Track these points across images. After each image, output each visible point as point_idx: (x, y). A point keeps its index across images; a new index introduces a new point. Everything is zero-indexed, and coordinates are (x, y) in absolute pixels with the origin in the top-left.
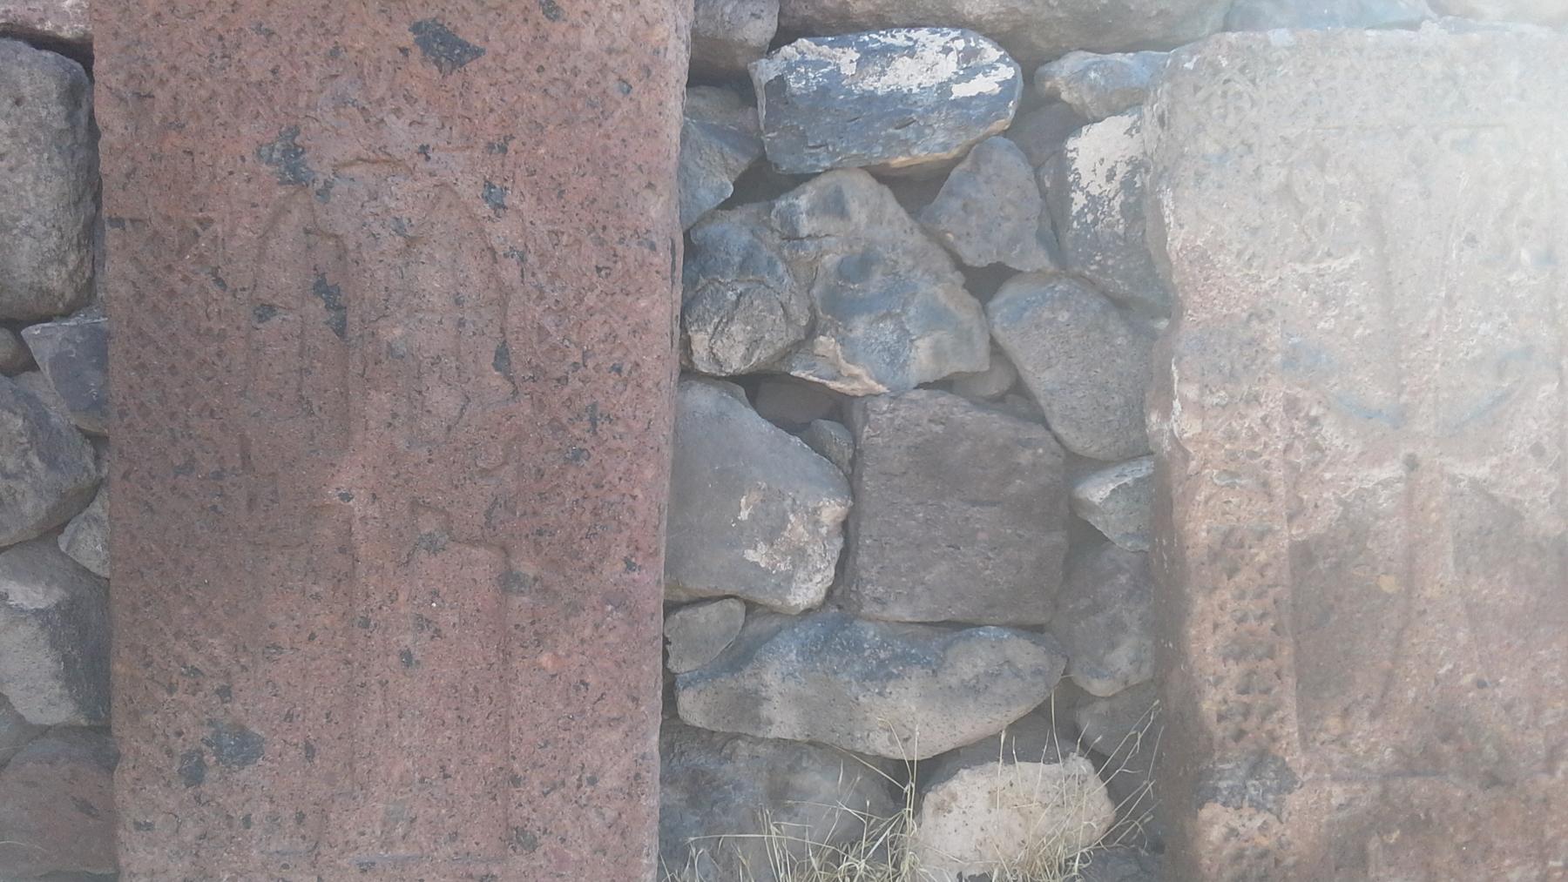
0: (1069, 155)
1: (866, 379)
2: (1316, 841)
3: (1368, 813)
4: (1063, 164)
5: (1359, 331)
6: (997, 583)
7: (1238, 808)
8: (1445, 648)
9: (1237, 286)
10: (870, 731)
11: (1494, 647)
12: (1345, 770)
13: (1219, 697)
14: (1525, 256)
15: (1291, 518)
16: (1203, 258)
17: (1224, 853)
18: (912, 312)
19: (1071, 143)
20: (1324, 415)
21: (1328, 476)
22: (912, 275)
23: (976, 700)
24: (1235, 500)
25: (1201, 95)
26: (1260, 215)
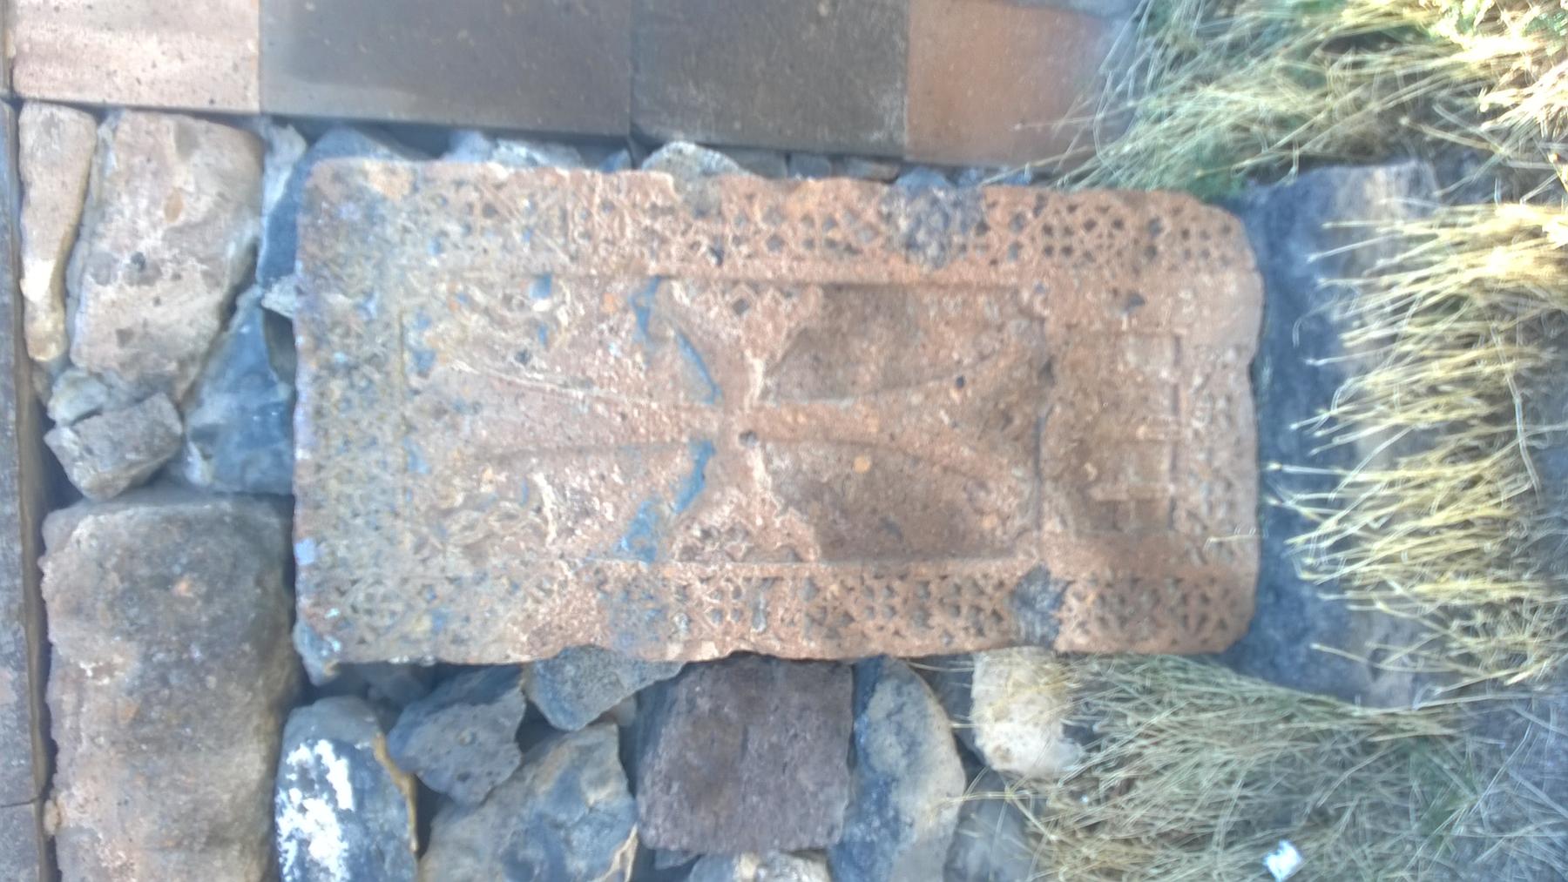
5: (616, 477)
6: (819, 728)
7: (1061, 622)
13: (962, 634)
14: (541, 306)
15: (798, 558)
16: (540, 635)
18: (562, 817)
21: (759, 522)
23: (920, 744)
25: (369, 637)
26: (499, 578)
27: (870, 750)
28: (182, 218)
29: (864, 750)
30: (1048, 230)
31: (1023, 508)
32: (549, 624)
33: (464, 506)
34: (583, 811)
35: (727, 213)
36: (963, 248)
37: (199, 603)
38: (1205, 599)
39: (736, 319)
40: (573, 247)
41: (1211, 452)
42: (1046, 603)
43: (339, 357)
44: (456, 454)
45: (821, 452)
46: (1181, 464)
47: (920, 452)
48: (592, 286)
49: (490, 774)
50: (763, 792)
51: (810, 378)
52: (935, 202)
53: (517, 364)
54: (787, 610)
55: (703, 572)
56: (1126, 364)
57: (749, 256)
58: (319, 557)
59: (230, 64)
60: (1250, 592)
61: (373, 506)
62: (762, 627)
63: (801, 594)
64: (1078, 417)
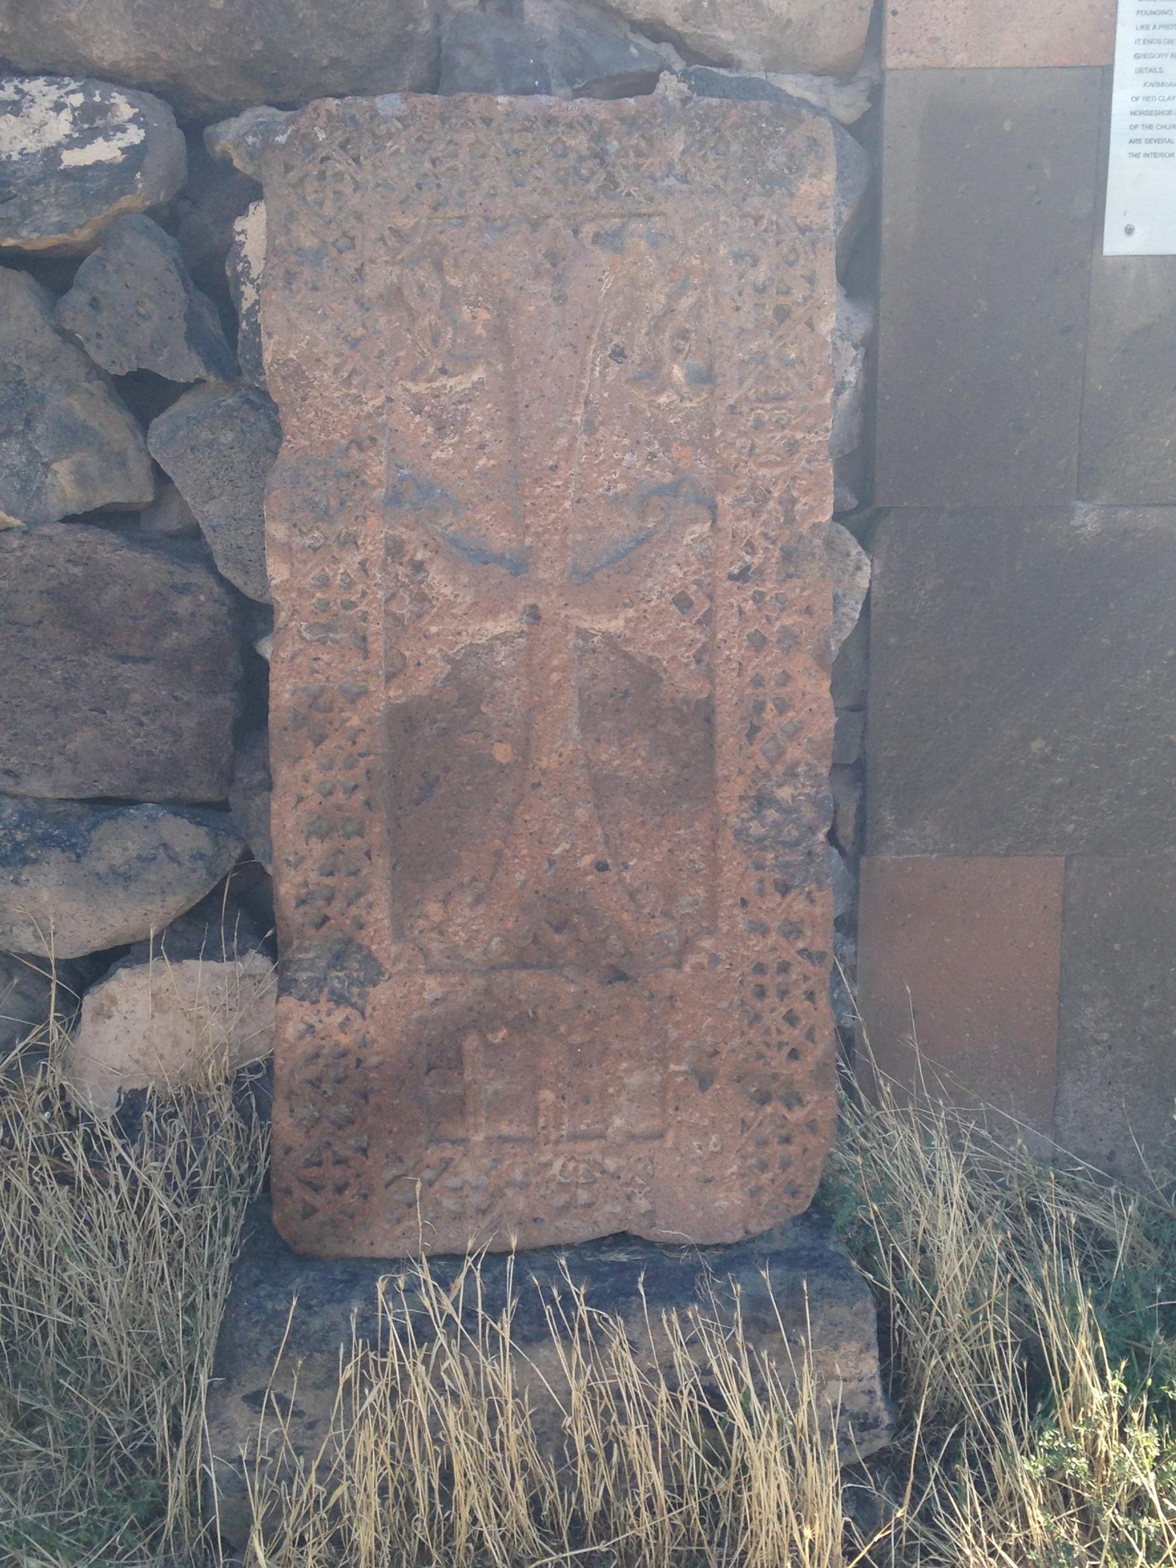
0: (238, 238)
2: (404, 1039)
3: (471, 1009)
4: (229, 248)
5: (482, 462)
6: (150, 753)
9: (335, 407)
10: (12, 925)
12: (446, 961)
13: (299, 879)
14: (678, 373)
15: (390, 678)
16: (296, 374)
18: (40, 428)
19: (239, 224)
21: (434, 629)
22: (38, 384)
23: (126, 888)
24: (326, 657)
25: (293, 176)
26: (364, 326)
30: (784, 968)
32: (310, 384)
35: (788, 584)
36: (759, 867)
38: (340, 1190)
39: (669, 597)
40: (745, 409)
41: (524, 1186)
42: (337, 985)
43: (613, 145)
44: (505, 276)
46: (508, 1147)
49: (99, 335)
52: (812, 830)
53: (610, 347)
54: (329, 664)
56: (628, 1071)
57: (741, 612)
58: (386, 120)
59: (939, 34)
60: (349, 1250)
62: (308, 636)
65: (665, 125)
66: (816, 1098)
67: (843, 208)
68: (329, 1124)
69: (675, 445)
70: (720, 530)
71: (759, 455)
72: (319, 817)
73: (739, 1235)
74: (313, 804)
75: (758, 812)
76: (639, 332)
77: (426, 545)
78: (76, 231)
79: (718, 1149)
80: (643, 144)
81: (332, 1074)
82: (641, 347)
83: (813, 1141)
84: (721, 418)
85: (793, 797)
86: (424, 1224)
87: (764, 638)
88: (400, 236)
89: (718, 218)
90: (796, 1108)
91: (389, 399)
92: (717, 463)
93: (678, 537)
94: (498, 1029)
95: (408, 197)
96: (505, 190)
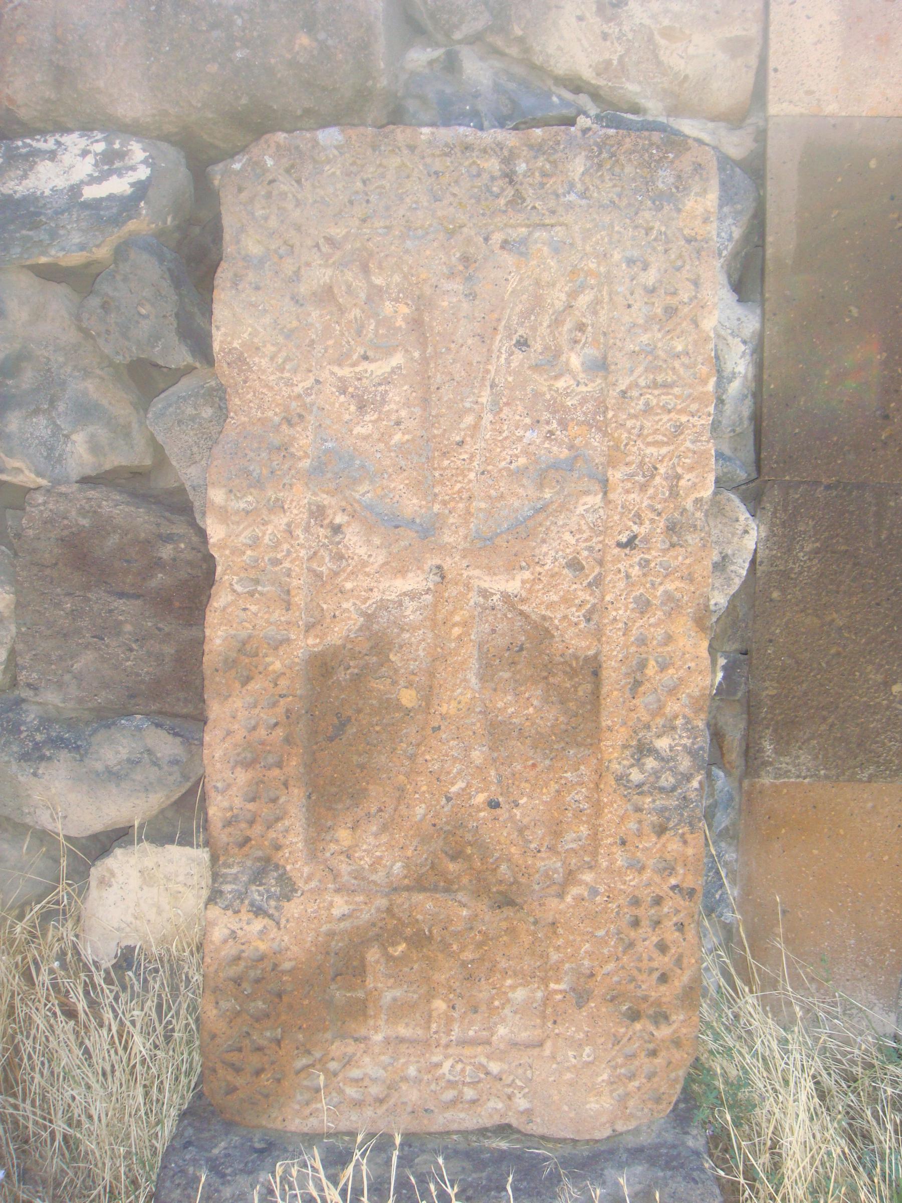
1: (27, 472)
2: (313, 949)
5: (398, 437)
6: (138, 675)
8: (458, 766)
9: (271, 388)
11: (518, 767)
12: (353, 881)
13: (226, 804)
14: (575, 361)
15: (309, 628)
17: (223, 953)
18: (61, 407)
20: (348, 523)
21: (349, 585)
22: (62, 371)
23: (118, 785)
25: (244, 196)
27: (113, 729)
28: (662, 42)
29: (114, 724)
30: (658, 901)
31: (358, 875)
32: (250, 369)
33: (372, 286)
34: (66, 427)
35: (672, 553)
37: (289, 56)
38: (258, 1073)
39: (563, 562)
40: (635, 393)
41: (418, 1081)
42: (256, 896)
43: (522, 167)
44: (423, 276)
45: (421, 653)
46: (403, 1048)
47: (420, 760)
48: (596, 413)
49: (108, 332)
50: (74, 614)
51: (502, 642)
52: (688, 778)
53: (515, 338)
54: (256, 615)
55: (297, 527)
56: (513, 988)
57: (628, 576)
61: (373, 198)
62: (238, 588)
63: (271, 631)
64: (456, 934)
65: (567, 151)
66: (681, 1017)
67: (733, 228)
68: (248, 1017)
69: (571, 424)
70: (610, 502)
71: (647, 436)
72: (244, 750)
73: (607, 1132)
74: (239, 737)
75: (639, 760)
76: (541, 324)
77: (344, 510)
78: (94, 249)
79: (591, 1059)
80: (548, 166)
81: (252, 974)
82: (543, 338)
83: (678, 1055)
84: (613, 401)
85: (671, 748)
86: (328, 1109)
87: (648, 601)
88: (333, 243)
89: (613, 227)
90: (663, 1027)
91: (318, 382)
92: (609, 441)
93: (572, 507)
94: (399, 943)
95: (341, 211)
96: (425, 204)
